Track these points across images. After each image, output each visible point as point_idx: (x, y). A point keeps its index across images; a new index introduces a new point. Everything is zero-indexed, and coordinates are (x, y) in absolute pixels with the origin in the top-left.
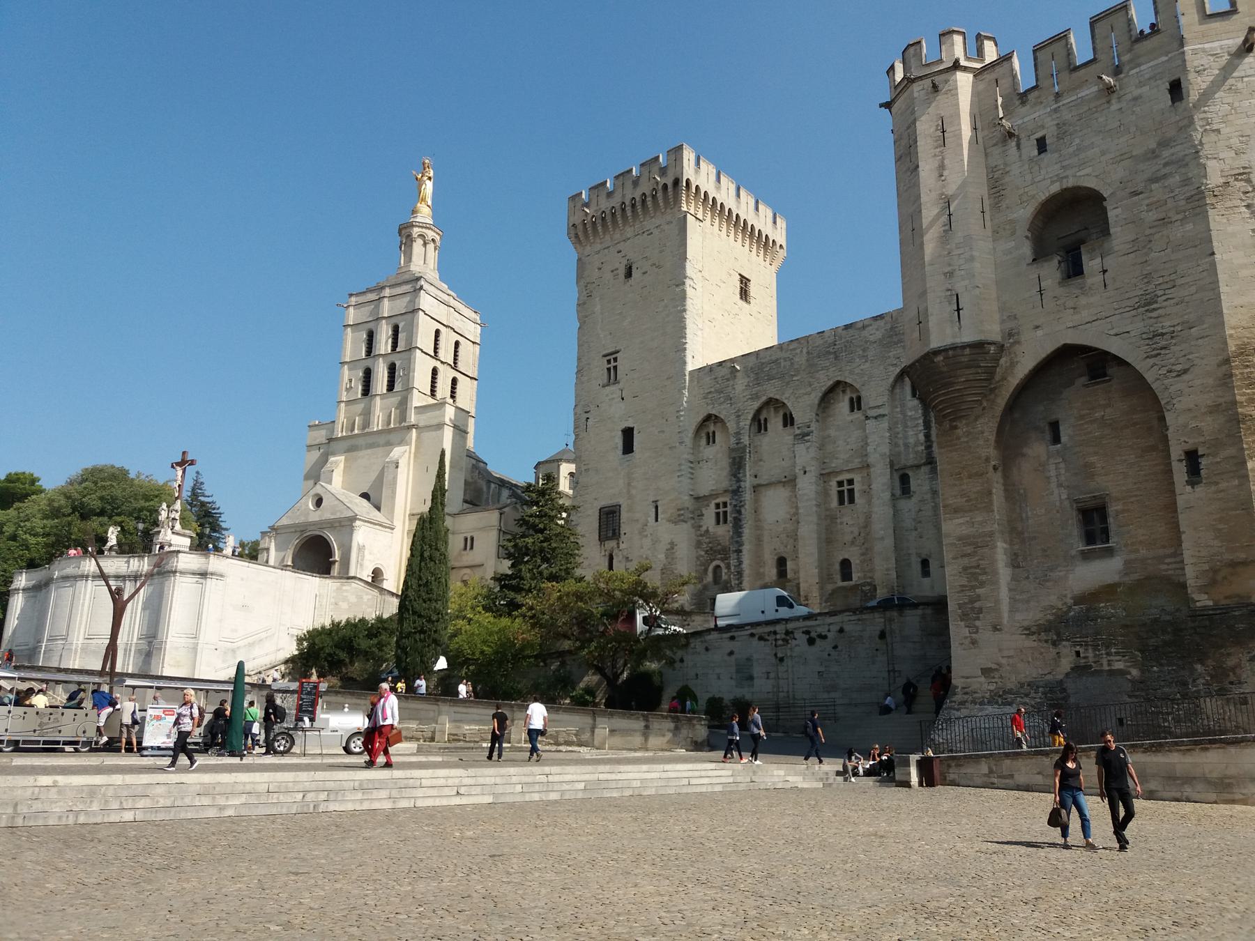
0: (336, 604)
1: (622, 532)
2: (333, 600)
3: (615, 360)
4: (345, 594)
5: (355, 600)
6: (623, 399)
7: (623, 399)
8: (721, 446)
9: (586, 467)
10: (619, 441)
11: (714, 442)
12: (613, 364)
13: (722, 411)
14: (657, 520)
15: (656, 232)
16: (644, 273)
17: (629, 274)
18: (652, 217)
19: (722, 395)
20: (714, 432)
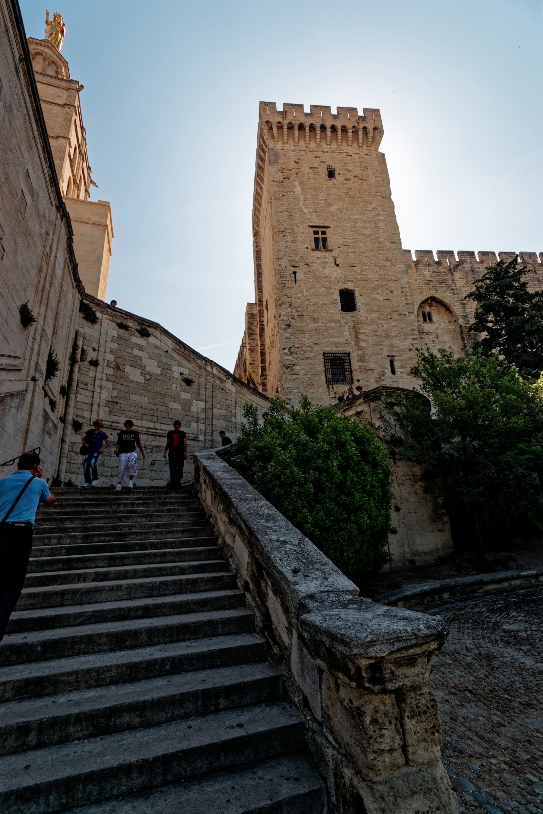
0: (117, 367)
1: (355, 378)
2: (111, 358)
3: (324, 233)
4: (136, 352)
5: (158, 371)
6: (338, 265)
7: (338, 265)
8: (440, 325)
9: (298, 313)
10: (337, 297)
11: (431, 320)
12: (320, 236)
13: (447, 297)
14: (393, 372)
15: (354, 155)
16: (346, 180)
17: (331, 174)
18: (349, 146)
19: (443, 285)
20: (429, 314)
